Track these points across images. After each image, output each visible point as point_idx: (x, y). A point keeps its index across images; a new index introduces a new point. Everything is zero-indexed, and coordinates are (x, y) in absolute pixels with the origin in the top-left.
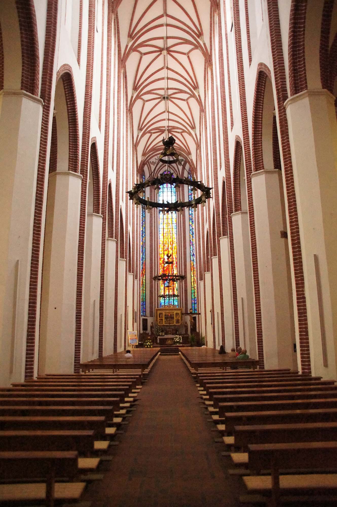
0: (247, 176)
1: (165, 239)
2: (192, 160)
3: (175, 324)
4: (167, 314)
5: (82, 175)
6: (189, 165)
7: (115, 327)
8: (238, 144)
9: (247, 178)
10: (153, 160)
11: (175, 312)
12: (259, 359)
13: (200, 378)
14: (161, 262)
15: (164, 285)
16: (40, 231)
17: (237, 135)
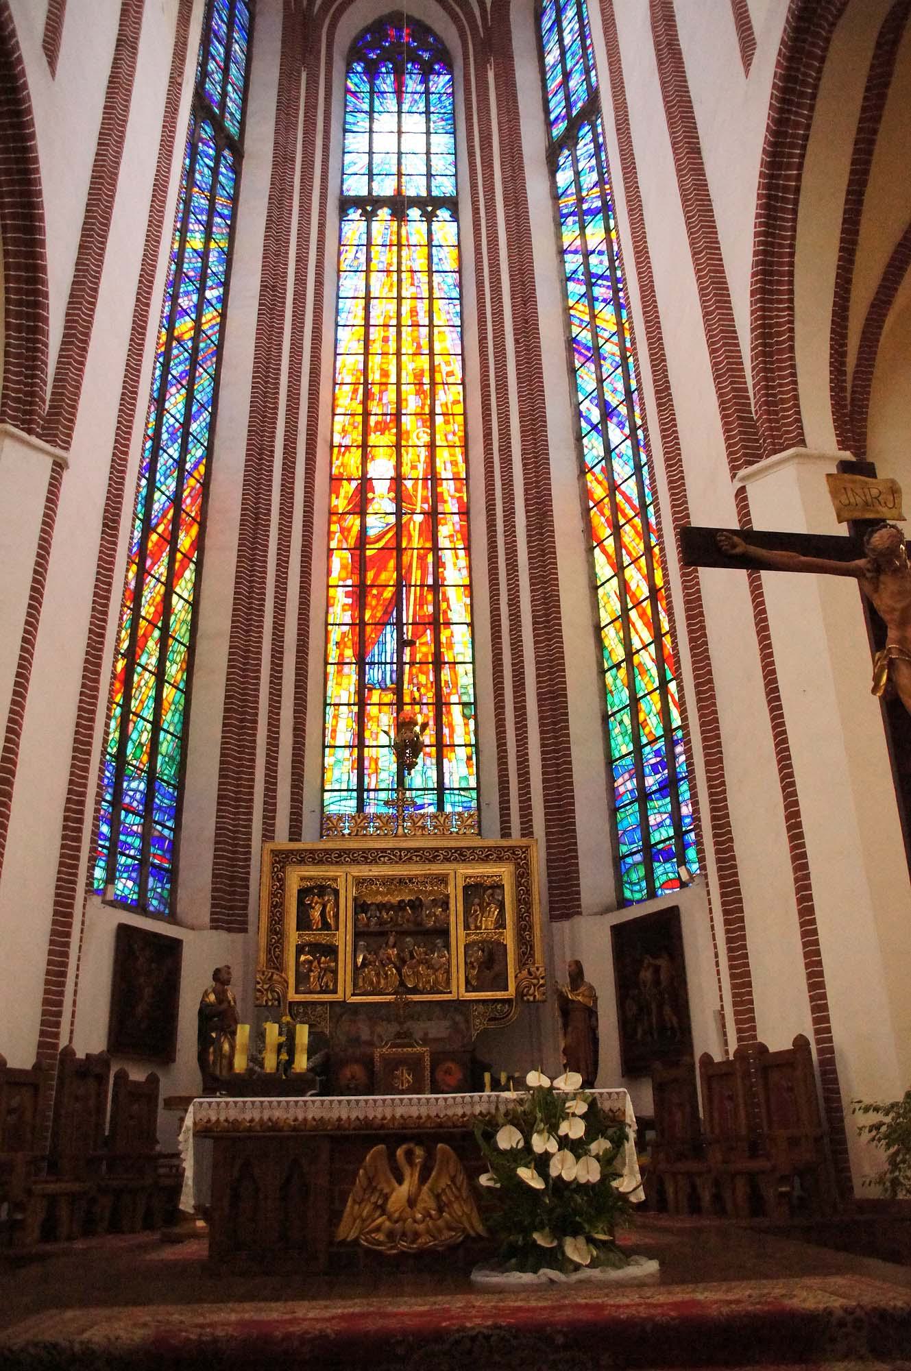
1: (375, 361)
3: (459, 990)
14: (341, 504)
15: (361, 674)
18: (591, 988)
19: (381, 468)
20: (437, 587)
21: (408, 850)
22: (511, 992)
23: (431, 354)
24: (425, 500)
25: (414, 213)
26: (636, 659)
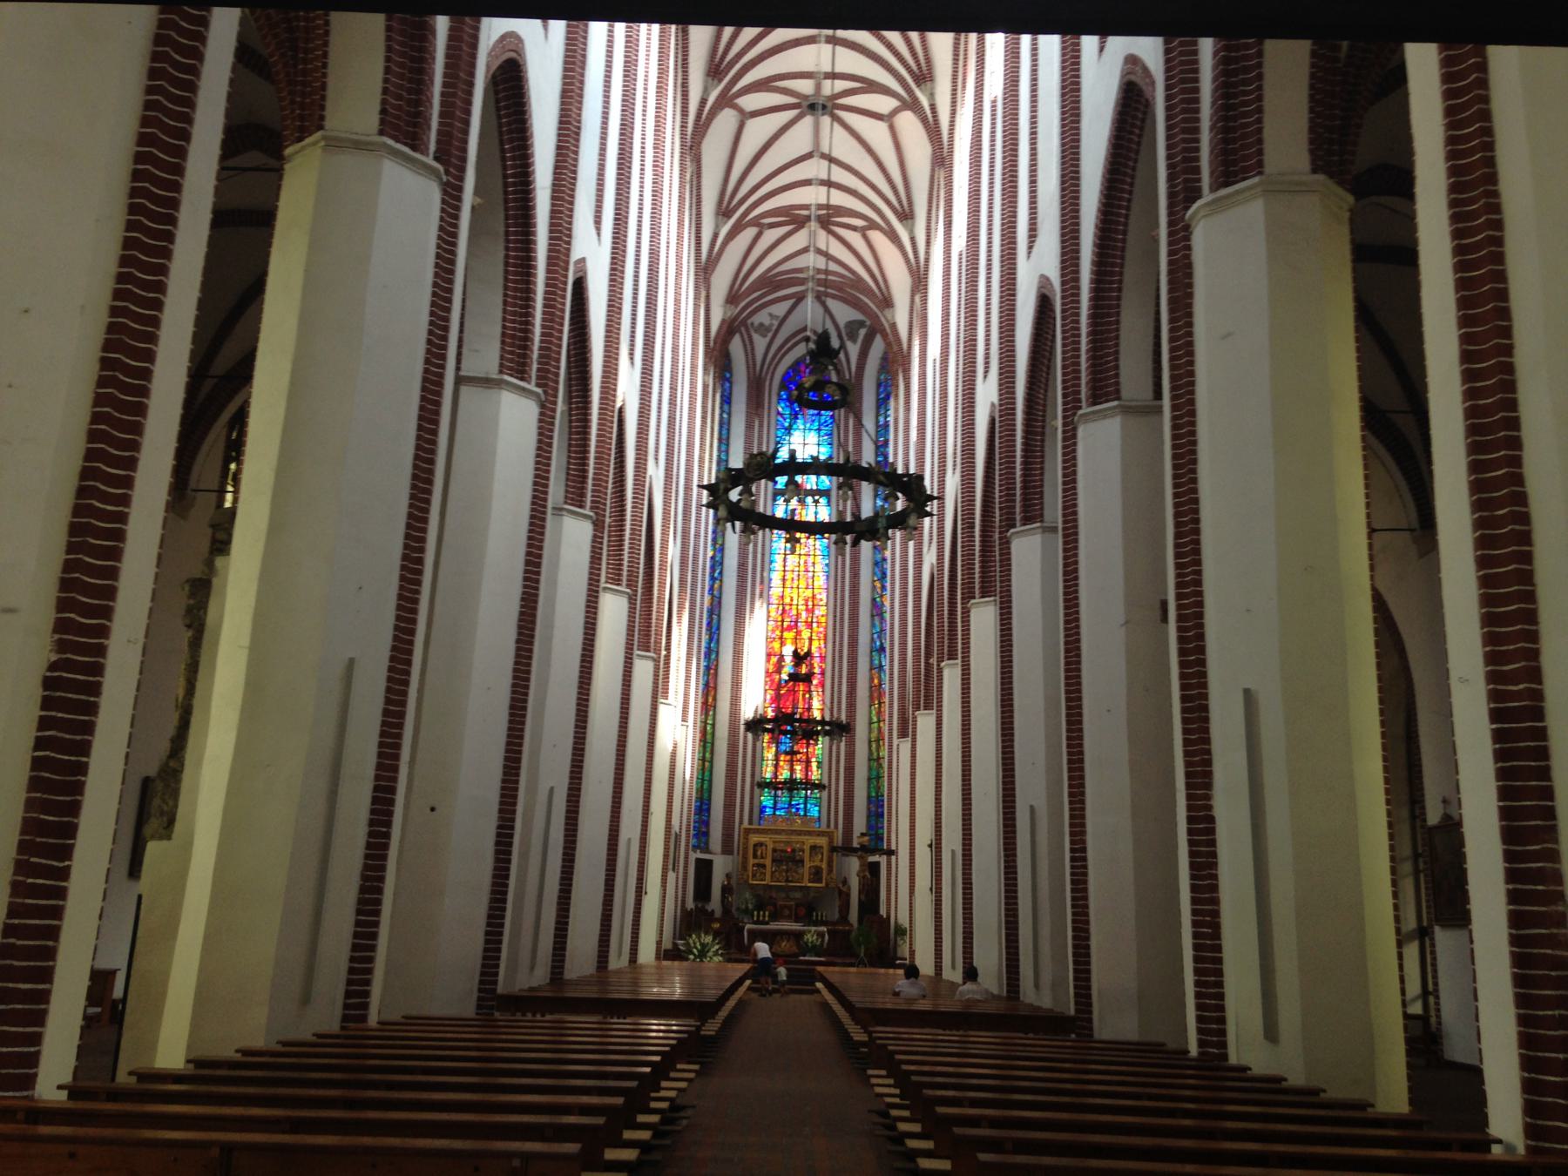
0: (1064, 417)
1: (787, 591)
2: (894, 326)
4: (780, 847)
5: (539, 390)
6: (885, 340)
7: (606, 880)
8: (1044, 305)
9: (1065, 425)
10: (762, 318)
11: (812, 840)
12: (1076, 1010)
13: (879, 1042)
15: (777, 747)
16: (420, 572)
17: (1042, 276)
25: (809, 500)
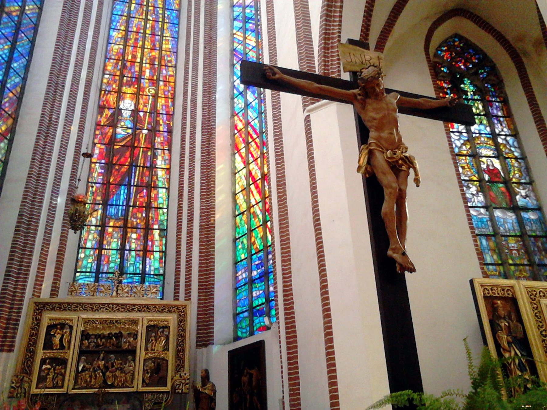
3: (138, 386)
15: (105, 210)
18: (213, 386)
19: (127, 104)
20: (153, 167)
21: (118, 305)
22: (168, 388)
23: (161, 49)
24: (149, 123)
26: (252, 210)
